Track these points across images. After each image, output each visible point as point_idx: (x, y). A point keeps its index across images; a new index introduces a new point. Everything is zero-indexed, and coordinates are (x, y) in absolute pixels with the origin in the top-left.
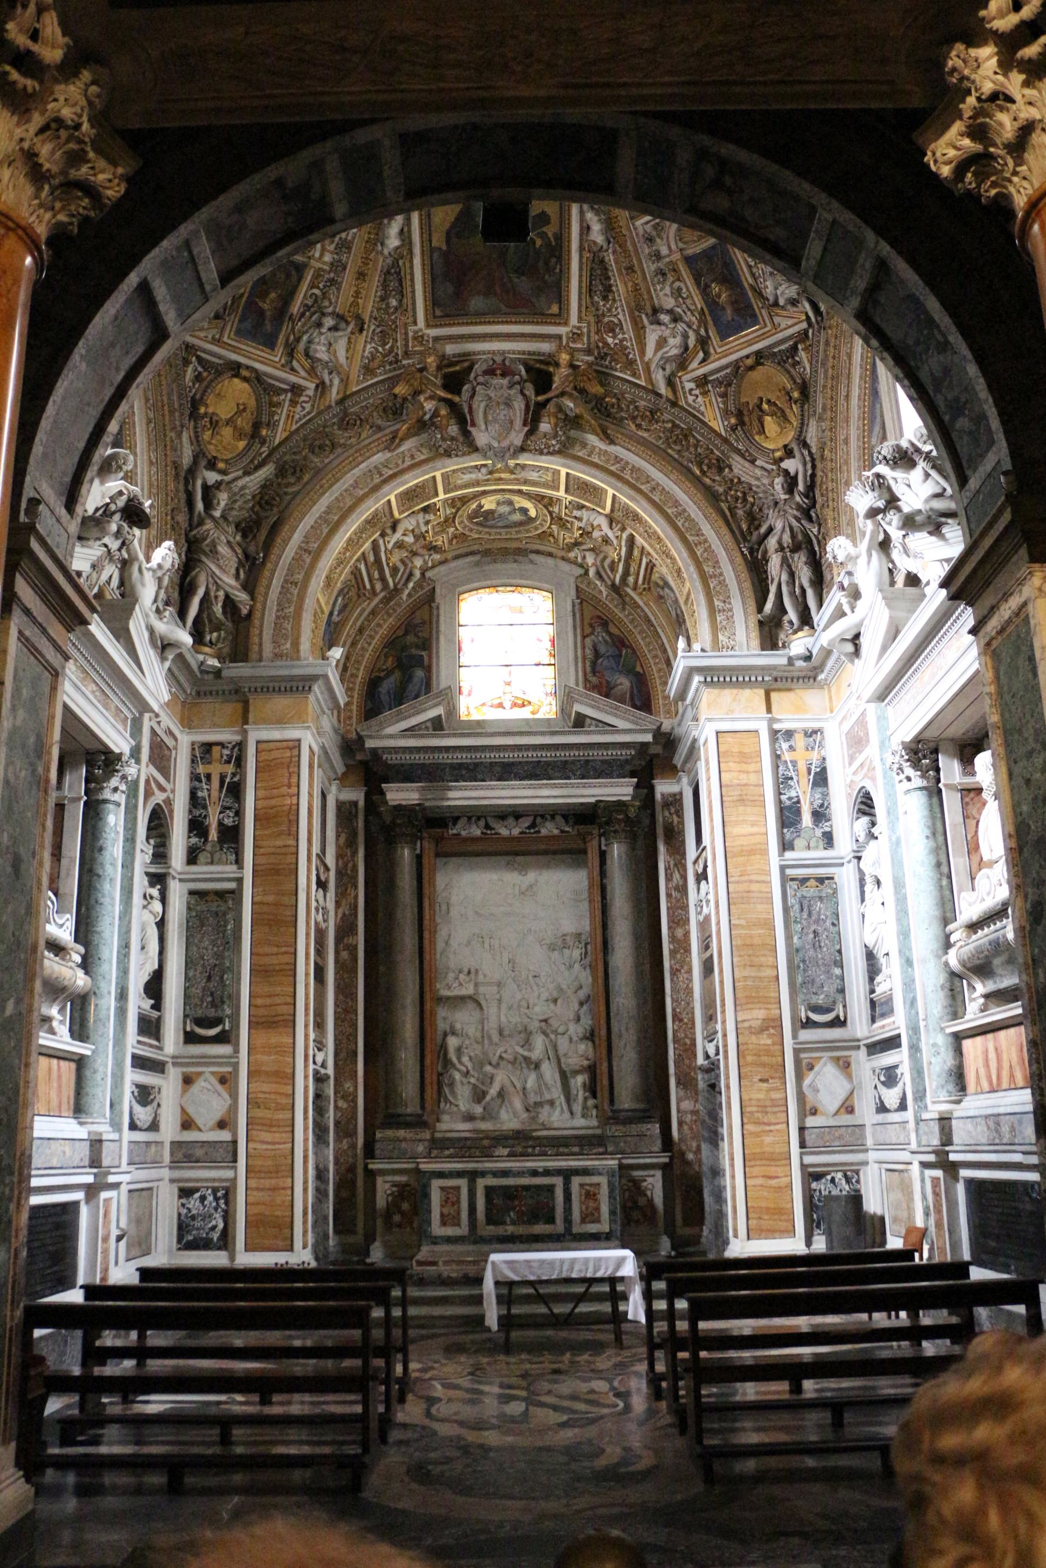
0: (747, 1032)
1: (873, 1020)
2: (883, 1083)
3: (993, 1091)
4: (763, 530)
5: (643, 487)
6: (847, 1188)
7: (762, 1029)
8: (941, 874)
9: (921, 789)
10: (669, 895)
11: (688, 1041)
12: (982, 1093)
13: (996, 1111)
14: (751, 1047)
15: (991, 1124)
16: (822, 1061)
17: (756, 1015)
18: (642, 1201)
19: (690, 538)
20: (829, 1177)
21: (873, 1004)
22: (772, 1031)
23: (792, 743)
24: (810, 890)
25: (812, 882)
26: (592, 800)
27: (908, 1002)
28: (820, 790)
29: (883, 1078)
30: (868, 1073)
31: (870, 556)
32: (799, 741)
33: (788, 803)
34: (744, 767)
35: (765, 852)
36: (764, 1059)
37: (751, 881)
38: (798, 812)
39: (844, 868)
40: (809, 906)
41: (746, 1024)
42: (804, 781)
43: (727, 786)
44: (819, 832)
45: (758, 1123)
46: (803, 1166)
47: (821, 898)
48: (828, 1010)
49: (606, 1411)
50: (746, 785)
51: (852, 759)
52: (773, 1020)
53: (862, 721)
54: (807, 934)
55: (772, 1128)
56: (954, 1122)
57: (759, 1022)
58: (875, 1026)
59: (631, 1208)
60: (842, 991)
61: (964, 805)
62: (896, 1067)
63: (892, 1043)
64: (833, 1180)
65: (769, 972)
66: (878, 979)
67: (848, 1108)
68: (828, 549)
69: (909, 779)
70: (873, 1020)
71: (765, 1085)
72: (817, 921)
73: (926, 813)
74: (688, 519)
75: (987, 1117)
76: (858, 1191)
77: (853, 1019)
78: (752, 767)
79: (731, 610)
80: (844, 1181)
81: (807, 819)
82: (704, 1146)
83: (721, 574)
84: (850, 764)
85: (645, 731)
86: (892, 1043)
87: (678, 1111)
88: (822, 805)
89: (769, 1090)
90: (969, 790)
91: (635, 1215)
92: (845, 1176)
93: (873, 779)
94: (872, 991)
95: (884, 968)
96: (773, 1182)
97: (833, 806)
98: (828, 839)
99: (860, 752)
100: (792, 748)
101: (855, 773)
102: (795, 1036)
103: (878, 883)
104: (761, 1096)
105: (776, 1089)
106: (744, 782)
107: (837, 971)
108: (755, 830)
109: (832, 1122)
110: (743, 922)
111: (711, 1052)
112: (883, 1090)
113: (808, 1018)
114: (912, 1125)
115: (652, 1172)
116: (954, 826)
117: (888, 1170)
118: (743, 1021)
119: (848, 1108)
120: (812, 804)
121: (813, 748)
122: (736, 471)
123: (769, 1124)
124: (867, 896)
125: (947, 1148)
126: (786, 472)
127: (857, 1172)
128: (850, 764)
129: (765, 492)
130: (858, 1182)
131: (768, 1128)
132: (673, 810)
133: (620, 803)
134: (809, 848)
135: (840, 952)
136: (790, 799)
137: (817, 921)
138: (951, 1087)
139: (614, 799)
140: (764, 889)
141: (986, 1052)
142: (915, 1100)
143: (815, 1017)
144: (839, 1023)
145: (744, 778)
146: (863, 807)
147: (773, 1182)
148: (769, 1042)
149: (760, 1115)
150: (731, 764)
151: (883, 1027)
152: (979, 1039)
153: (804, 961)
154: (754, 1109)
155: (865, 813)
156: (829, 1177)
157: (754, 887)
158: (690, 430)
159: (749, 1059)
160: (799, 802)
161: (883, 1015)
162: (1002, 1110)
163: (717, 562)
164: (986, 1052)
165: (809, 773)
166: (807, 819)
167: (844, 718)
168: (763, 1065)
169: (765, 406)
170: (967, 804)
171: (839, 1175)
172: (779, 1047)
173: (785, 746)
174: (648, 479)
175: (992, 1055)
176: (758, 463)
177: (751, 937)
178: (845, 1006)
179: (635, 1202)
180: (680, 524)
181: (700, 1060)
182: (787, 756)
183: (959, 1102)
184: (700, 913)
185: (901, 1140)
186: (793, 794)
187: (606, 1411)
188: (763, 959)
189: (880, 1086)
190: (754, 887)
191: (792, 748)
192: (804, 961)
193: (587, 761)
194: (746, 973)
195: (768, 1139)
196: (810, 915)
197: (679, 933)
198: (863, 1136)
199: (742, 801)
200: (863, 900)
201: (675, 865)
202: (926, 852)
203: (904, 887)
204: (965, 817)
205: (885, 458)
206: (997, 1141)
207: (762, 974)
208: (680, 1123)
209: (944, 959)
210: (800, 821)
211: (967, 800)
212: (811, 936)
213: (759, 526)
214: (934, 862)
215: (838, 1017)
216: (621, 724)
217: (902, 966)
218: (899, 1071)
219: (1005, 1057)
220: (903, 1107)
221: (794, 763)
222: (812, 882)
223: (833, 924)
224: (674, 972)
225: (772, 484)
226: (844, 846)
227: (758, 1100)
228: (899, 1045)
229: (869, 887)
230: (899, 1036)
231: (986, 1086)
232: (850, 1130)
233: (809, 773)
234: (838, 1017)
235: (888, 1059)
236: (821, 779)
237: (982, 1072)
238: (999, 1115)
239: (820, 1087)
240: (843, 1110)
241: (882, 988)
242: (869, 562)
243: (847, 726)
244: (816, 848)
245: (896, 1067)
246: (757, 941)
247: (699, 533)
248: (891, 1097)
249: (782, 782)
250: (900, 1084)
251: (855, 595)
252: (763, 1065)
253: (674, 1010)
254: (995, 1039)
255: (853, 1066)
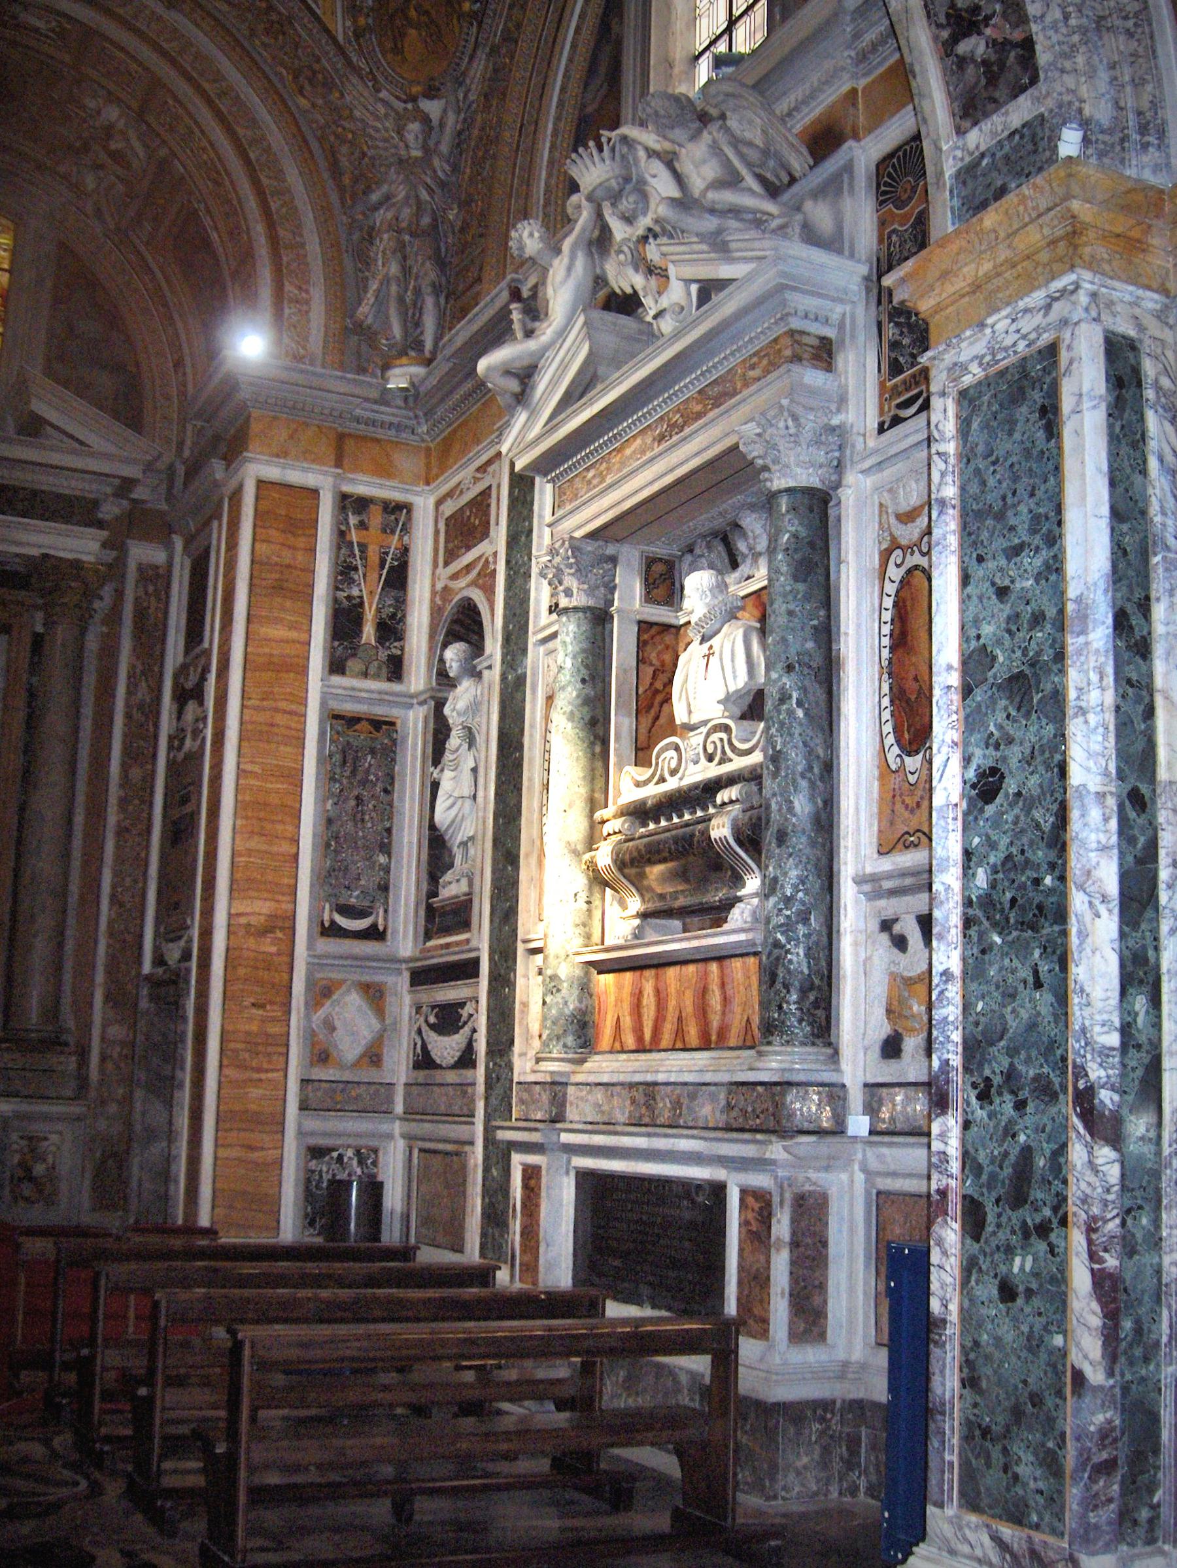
0: (242, 932)
1: (428, 936)
2: (432, 1027)
3: (641, 1049)
4: (375, 197)
5: (206, 86)
6: (359, 1171)
7: (265, 931)
8: (596, 737)
9: (584, 610)
10: (128, 716)
11: (129, 938)
12: (623, 1051)
13: (649, 1078)
14: (246, 954)
15: (640, 1098)
16: (344, 988)
17: (259, 908)
18: (39, 1169)
19: (265, 181)
20: (335, 1154)
21: (431, 911)
22: (279, 935)
23: (364, 517)
24: (360, 737)
25: (365, 725)
26: (35, 552)
27: (498, 914)
28: (394, 593)
29: (432, 1020)
30: (407, 1010)
31: (573, 258)
32: (376, 518)
33: (346, 603)
34: (291, 540)
35: (304, 671)
36: (266, 975)
37: (276, 710)
38: (358, 621)
39: (411, 713)
40: (356, 759)
41: (243, 920)
42: (373, 576)
43: (261, 563)
44: (383, 655)
45: (243, 1067)
46: (301, 1133)
47: (373, 752)
48: (361, 914)
49: (64, 1492)
50: (288, 566)
51: (451, 557)
52: (285, 918)
53: (481, 503)
54: (347, 799)
55: (263, 1076)
56: (571, 1090)
57: (262, 918)
58: (430, 944)
59: (20, 1180)
60: (385, 888)
61: (641, 645)
62: (462, 1005)
63: (468, 969)
64: (340, 1157)
65: (286, 848)
66: (448, 876)
67: (373, 1056)
68: (513, 234)
69: (568, 593)
70: (428, 936)
71: (260, 1012)
72: (364, 783)
73: (585, 645)
74: (268, 150)
75: (632, 1086)
76: (374, 1176)
77: (395, 932)
78: (301, 542)
79: (307, 302)
80: (355, 1162)
81: (369, 632)
82: (139, 1094)
83: (303, 245)
84: (446, 564)
85: (135, 461)
86: (468, 969)
87: (103, 1039)
88: (393, 616)
89: (263, 1021)
90: (651, 624)
91: (27, 1189)
92: (358, 1152)
93: (489, 591)
94: (433, 893)
95: (458, 861)
96: (255, 1155)
97: (409, 620)
98: (396, 669)
99: (469, 548)
100: (362, 525)
101: (455, 577)
102: (310, 946)
103: (471, 739)
104: (254, 1028)
105: (274, 1020)
106: (287, 561)
107: (382, 859)
108: (293, 635)
109: (347, 1076)
110: (256, 768)
111: (173, 953)
112: (432, 1038)
113: (333, 922)
114: (481, 1088)
115: (59, 1127)
116: (623, 670)
117: (421, 1150)
118: (239, 915)
119: (373, 1056)
120: (379, 610)
121: (393, 532)
122: (348, 98)
123: (259, 1070)
124: (448, 756)
125: (559, 1125)
126: (426, 120)
127: (375, 1151)
128: (446, 564)
129: (386, 140)
130: (375, 1163)
131: (256, 1076)
132: (151, 589)
133: (76, 564)
134: (365, 675)
135: (389, 831)
136: (349, 598)
137: (364, 783)
138: (570, 1040)
139: (70, 556)
140: (293, 725)
141: (638, 996)
142: (490, 1053)
143: (338, 919)
144: (375, 934)
145: (287, 556)
146: (457, 627)
147: (255, 1155)
148: (273, 949)
149: (247, 1055)
150: (273, 532)
151: (448, 946)
152: (628, 976)
153: (337, 838)
154: (240, 1046)
155: (459, 638)
156: (335, 1154)
157: (280, 719)
158: (290, 20)
159: (242, 971)
160: (361, 604)
161: (447, 931)
162: (661, 1078)
163: (299, 226)
164: (638, 996)
165: (382, 567)
166: (369, 632)
167: (450, 494)
168: (259, 982)
169: (413, 13)
170: (645, 643)
171: (350, 1153)
172: (286, 959)
173: (353, 520)
174: (218, 77)
175: (649, 1001)
176: (383, 94)
177: (268, 792)
178: (386, 911)
179: (29, 1170)
180: (252, 156)
181: (147, 968)
182: (354, 536)
183: (582, 1061)
184: (180, 748)
185: (465, 1111)
186: (355, 592)
187: (64, 1492)
188: (280, 827)
189: (425, 1028)
190: (280, 719)
191: (362, 525)
192: (337, 838)
193: (35, 493)
194: (253, 844)
195: (255, 1092)
196: (354, 772)
197: (136, 773)
198: (390, 1100)
199: (279, 588)
200: (437, 761)
201: (143, 673)
202: (579, 701)
203: (520, 747)
204: (640, 661)
205: (656, 113)
206: (646, 1120)
207: (275, 849)
208: (104, 1058)
209: (587, 856)
210: (358, 632)
211: (646, 637)
212: (353, 803)
213: (367, 191)
214: (587, 718)
215: (374, 926)
216: (93, 440)
217: (495, 861)
218: (465, 1013)
219: (672, 1003)
220: (466, 1060)
221: (363, 547)
222: (365, 725)
223: (386, 791)
224: (121, 832)
225: (400, 131)
226: (418, 677)
227: (248, 1033)
228: (476, 974)
229: (454, 741)
230: (476, 962)
231: (630, 1041)
232: (373, 1087)
233: (382, 565)
234: (374, 926)
235: (449, 993)
236: (398, 578)
237: (627, 1022)
238: (655, 1084)
239: (337, 1023)
240: (366, 1059)
241: (452, 888)
242: (569, 269)
243: (449, 508)
244: (377, 677)
245: (462, 1005)
246: (274, 799)
247: (279, 175)
248: (446, 1048)
249: (344, 572)
250: (466, 1030)
251: (535, 311)
252: (259, 982)
253: (114, 887)
254: (657, 977)
255: (389, 999)
